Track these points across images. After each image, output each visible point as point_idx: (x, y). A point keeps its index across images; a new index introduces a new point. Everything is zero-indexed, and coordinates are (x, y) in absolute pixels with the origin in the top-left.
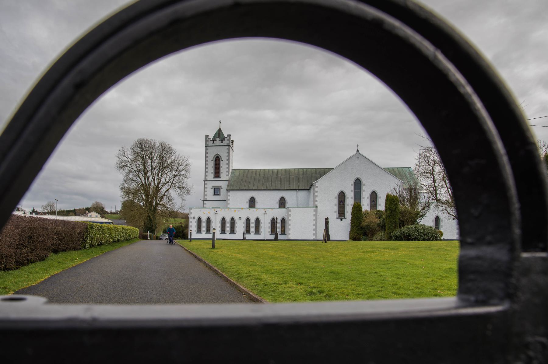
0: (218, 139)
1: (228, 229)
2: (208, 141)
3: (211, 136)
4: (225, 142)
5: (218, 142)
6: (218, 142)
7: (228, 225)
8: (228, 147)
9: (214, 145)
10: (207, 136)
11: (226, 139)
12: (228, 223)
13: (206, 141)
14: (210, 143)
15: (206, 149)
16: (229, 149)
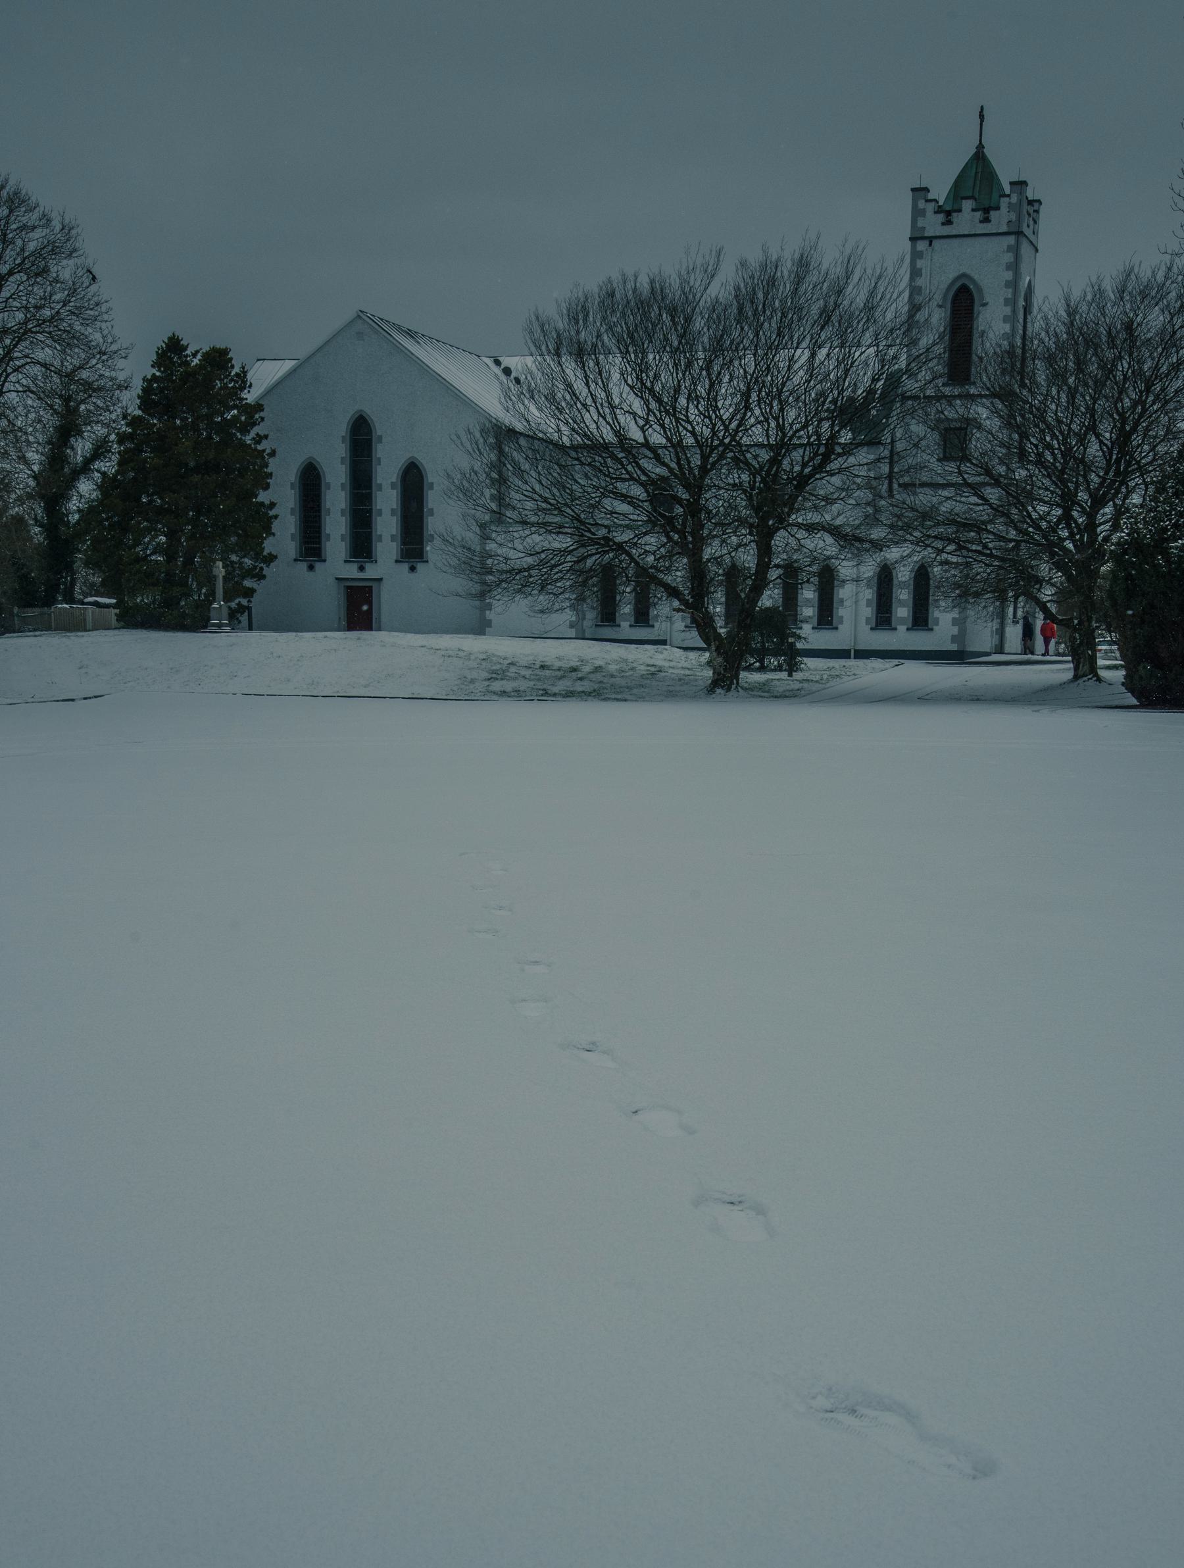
0: (967, 205)
1: (902, 612)
2: (922, 213)
3: (941, 192)
4: (1001, 219)
5: (967, 219)
6: (967, 219)
7: (903, 596)
8: (1011, 240)
9: (947, 230)
10: (920, 192)
11: (1004, 202)
12: (903, 585)
13: (917, 213)
14: (932, 224)
15: (916, 255)
16: (1016, 250)
